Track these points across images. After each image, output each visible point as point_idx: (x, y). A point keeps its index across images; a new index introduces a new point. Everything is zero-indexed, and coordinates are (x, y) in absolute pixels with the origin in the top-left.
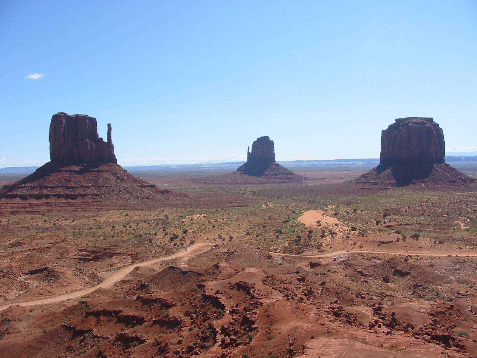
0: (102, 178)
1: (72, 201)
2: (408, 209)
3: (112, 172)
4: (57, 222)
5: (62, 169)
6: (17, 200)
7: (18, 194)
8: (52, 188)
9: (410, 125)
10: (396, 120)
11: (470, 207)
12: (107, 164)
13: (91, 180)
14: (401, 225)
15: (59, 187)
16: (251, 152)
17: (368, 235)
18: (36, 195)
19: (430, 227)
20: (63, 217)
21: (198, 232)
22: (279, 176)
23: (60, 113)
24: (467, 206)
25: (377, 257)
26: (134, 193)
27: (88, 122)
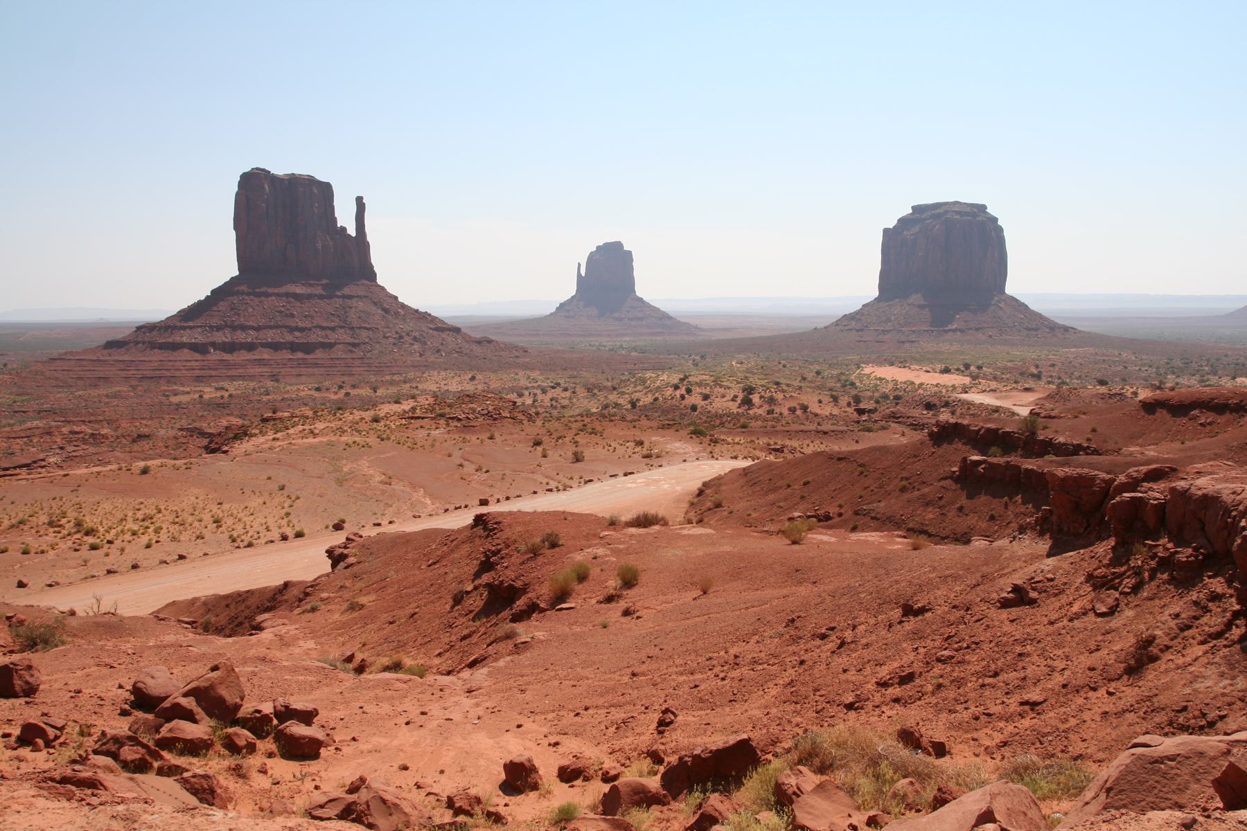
0: (353, 310)
1: (307, 356)
3: (371, 299)
5: (270, 290)
6: (186, 354)
7: (185, 341)
8: (258, 329)
9: (948, 216)
10: (913, 208)
12: (359, 283)
13: (332, 314)
15: (271, 327)
16: (583, 275)
18: (224, 343)
22: (644, 323)
23: (257, 169)
26: (429, 343)
27: (316, 191)
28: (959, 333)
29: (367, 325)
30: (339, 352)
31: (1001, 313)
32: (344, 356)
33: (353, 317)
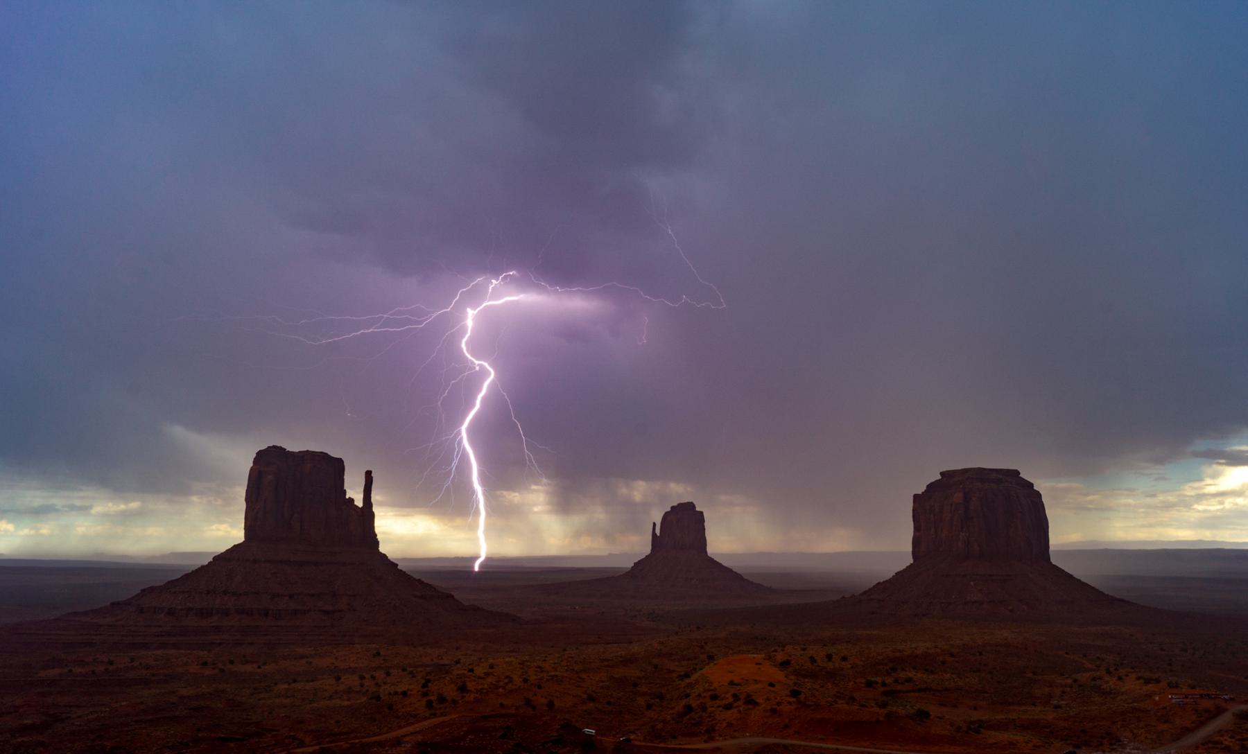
10: (941, 473)
16: (658, 534)
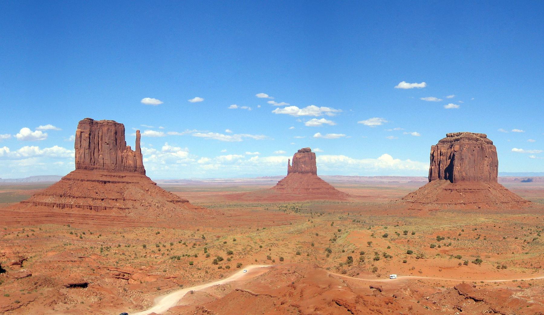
2: (462, 233)
4: (84, 235)
10: (447, 135)
11: (526, 230)
14: (457, 250)
17: (427, 259)
19: (488, 252)
20: (89, 231)
21: (245, 254)
23: (87, 119)
24: (522, 228)
25: (439, 284)
28: (463, 205)
29: (133, 199)
30: (113, 213)
31: (489, 194)
32: (115, 215)
33: (126, 194)
